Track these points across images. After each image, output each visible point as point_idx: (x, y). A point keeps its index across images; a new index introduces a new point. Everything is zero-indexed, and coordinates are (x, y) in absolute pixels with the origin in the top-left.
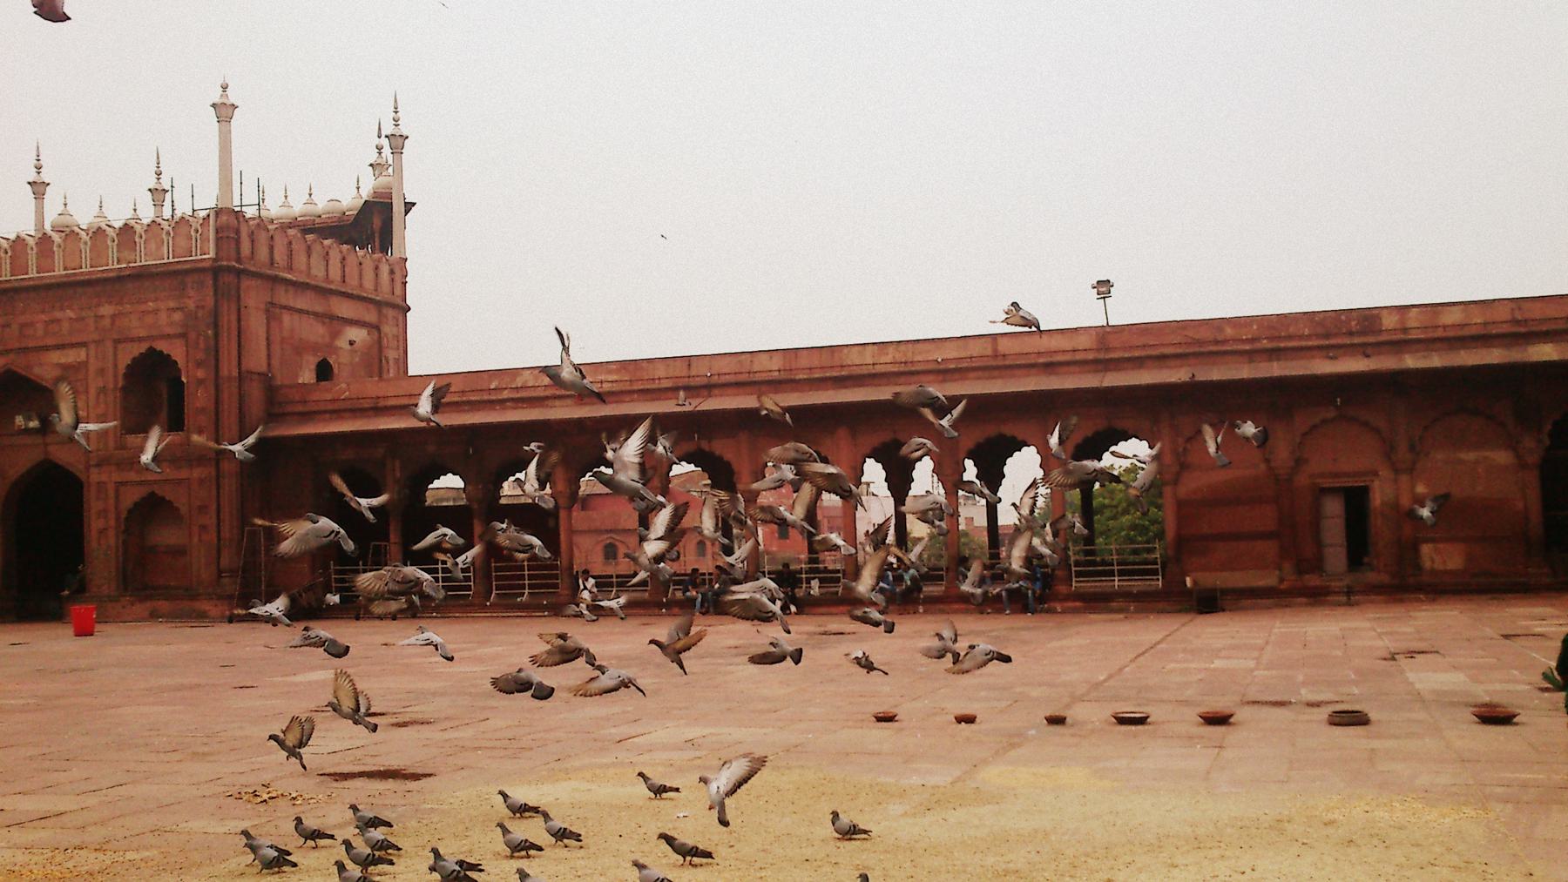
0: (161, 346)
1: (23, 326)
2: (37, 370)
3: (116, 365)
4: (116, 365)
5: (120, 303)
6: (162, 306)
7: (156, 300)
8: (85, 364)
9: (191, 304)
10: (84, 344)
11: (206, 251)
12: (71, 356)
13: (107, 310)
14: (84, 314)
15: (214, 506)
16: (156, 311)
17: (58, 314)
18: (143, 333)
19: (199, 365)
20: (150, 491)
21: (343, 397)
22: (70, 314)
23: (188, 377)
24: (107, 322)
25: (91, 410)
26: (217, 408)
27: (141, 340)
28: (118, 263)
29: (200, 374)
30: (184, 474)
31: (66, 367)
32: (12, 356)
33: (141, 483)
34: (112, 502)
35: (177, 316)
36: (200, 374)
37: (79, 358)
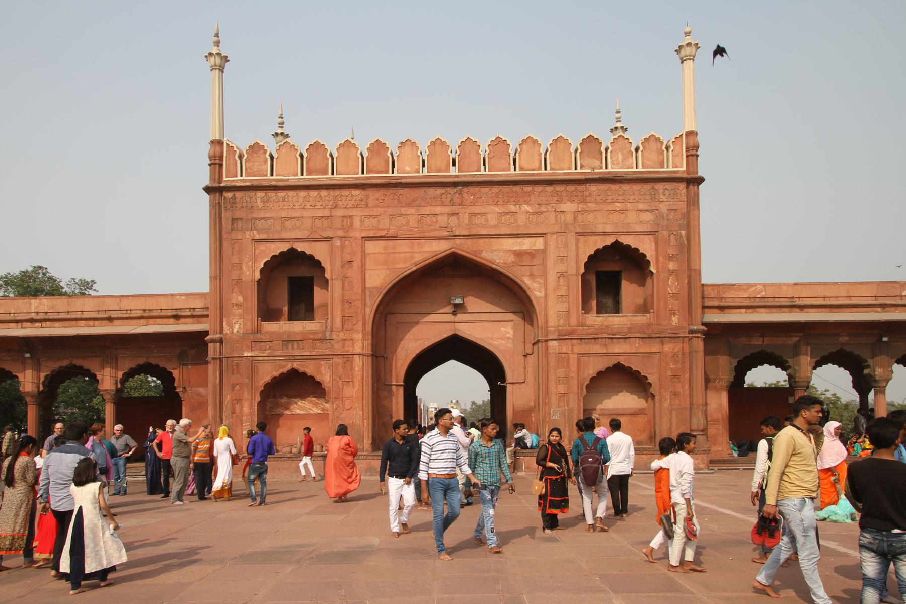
0: (625, 240)
1: (475, 215)
2: (484, 255)
3: (577, 254)
4: (577, 254)
5: (584, 202)
6: (629, 206)
7: (625, 201)
8: (544, 251)
9: (663, 208)
10: (542, 235)
11: (678, 164)
12: (526, 244)
13: (569, 207)
14: (543, 209)
15: (687, 376)
16: (623, 211)
17: (512, 208)
18: (609, 229)
19: (671, 258)
20: (616, 362)
21: (759, 296)
22: (526, 208)
23: (657, 269)
24: (569, 218)
25: (550, 291)
26: (689, 294)
27: (605, 234)
28: (581, 168)
29: (672, 266)
30: (655, 347)
31: (519, 254)
32: (458, 241)
33: (606, 355)
34: (574, 368)
35: (648, 217)
36: (672, 266)
37: (534, 246)
